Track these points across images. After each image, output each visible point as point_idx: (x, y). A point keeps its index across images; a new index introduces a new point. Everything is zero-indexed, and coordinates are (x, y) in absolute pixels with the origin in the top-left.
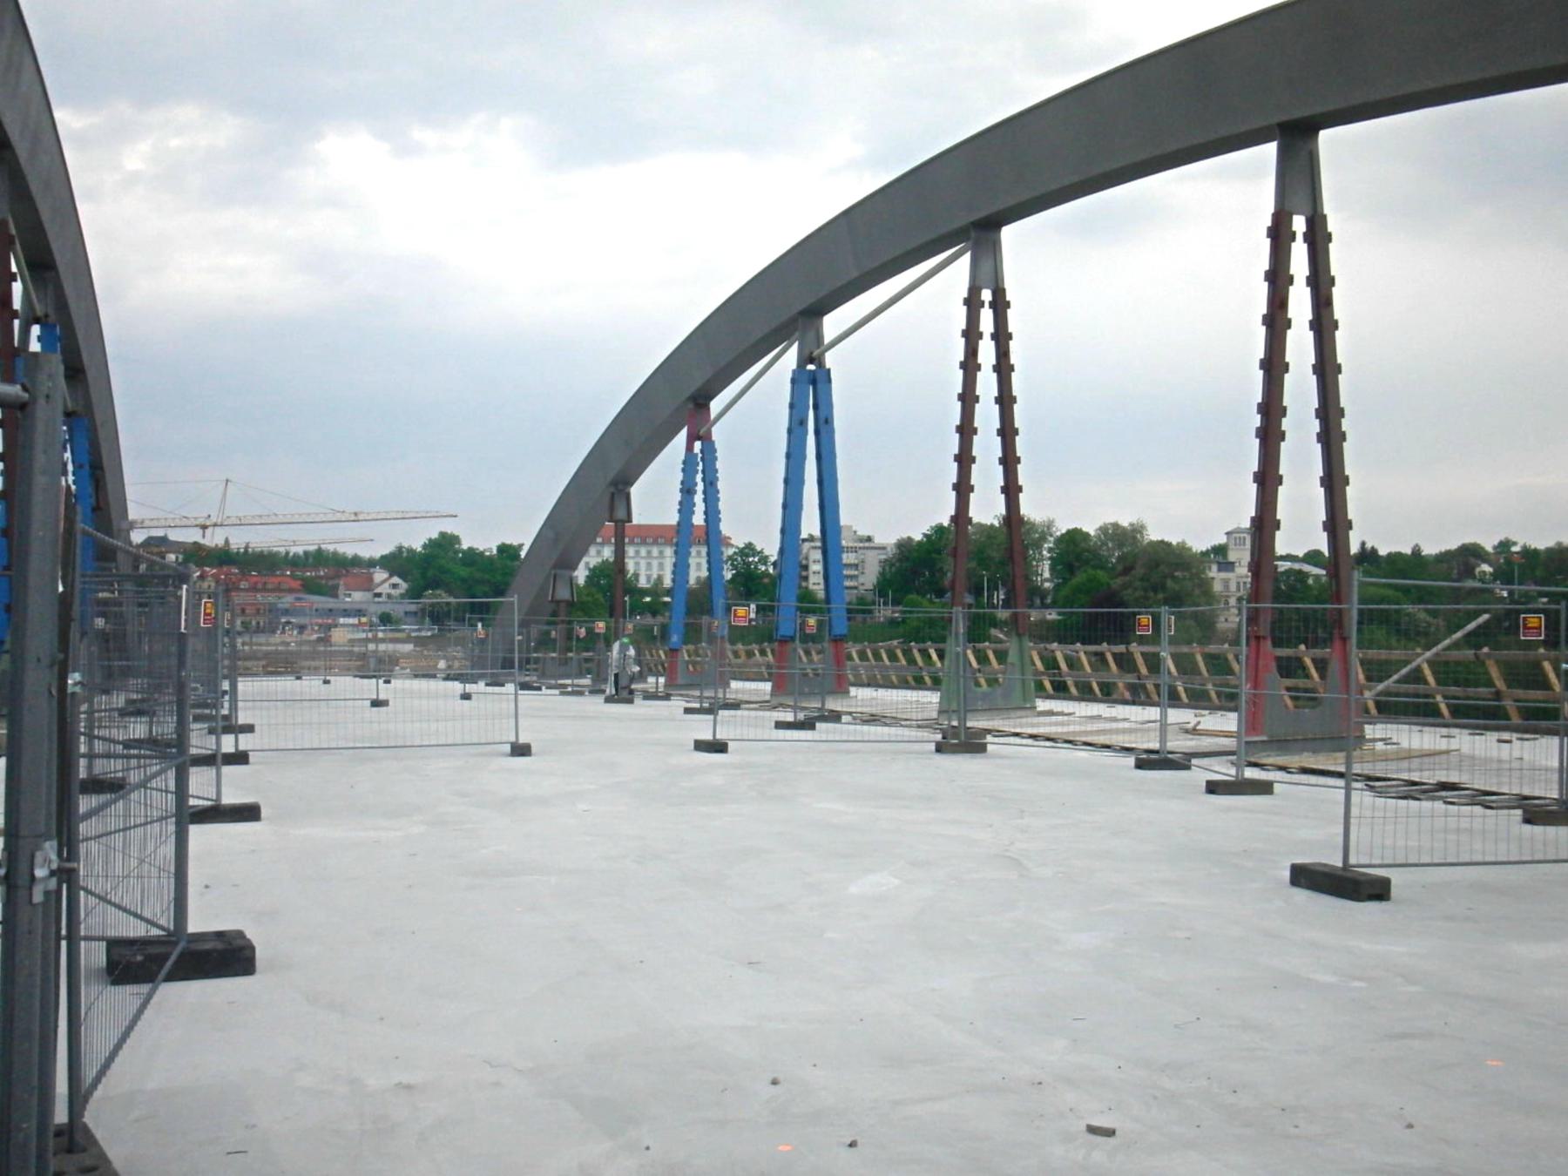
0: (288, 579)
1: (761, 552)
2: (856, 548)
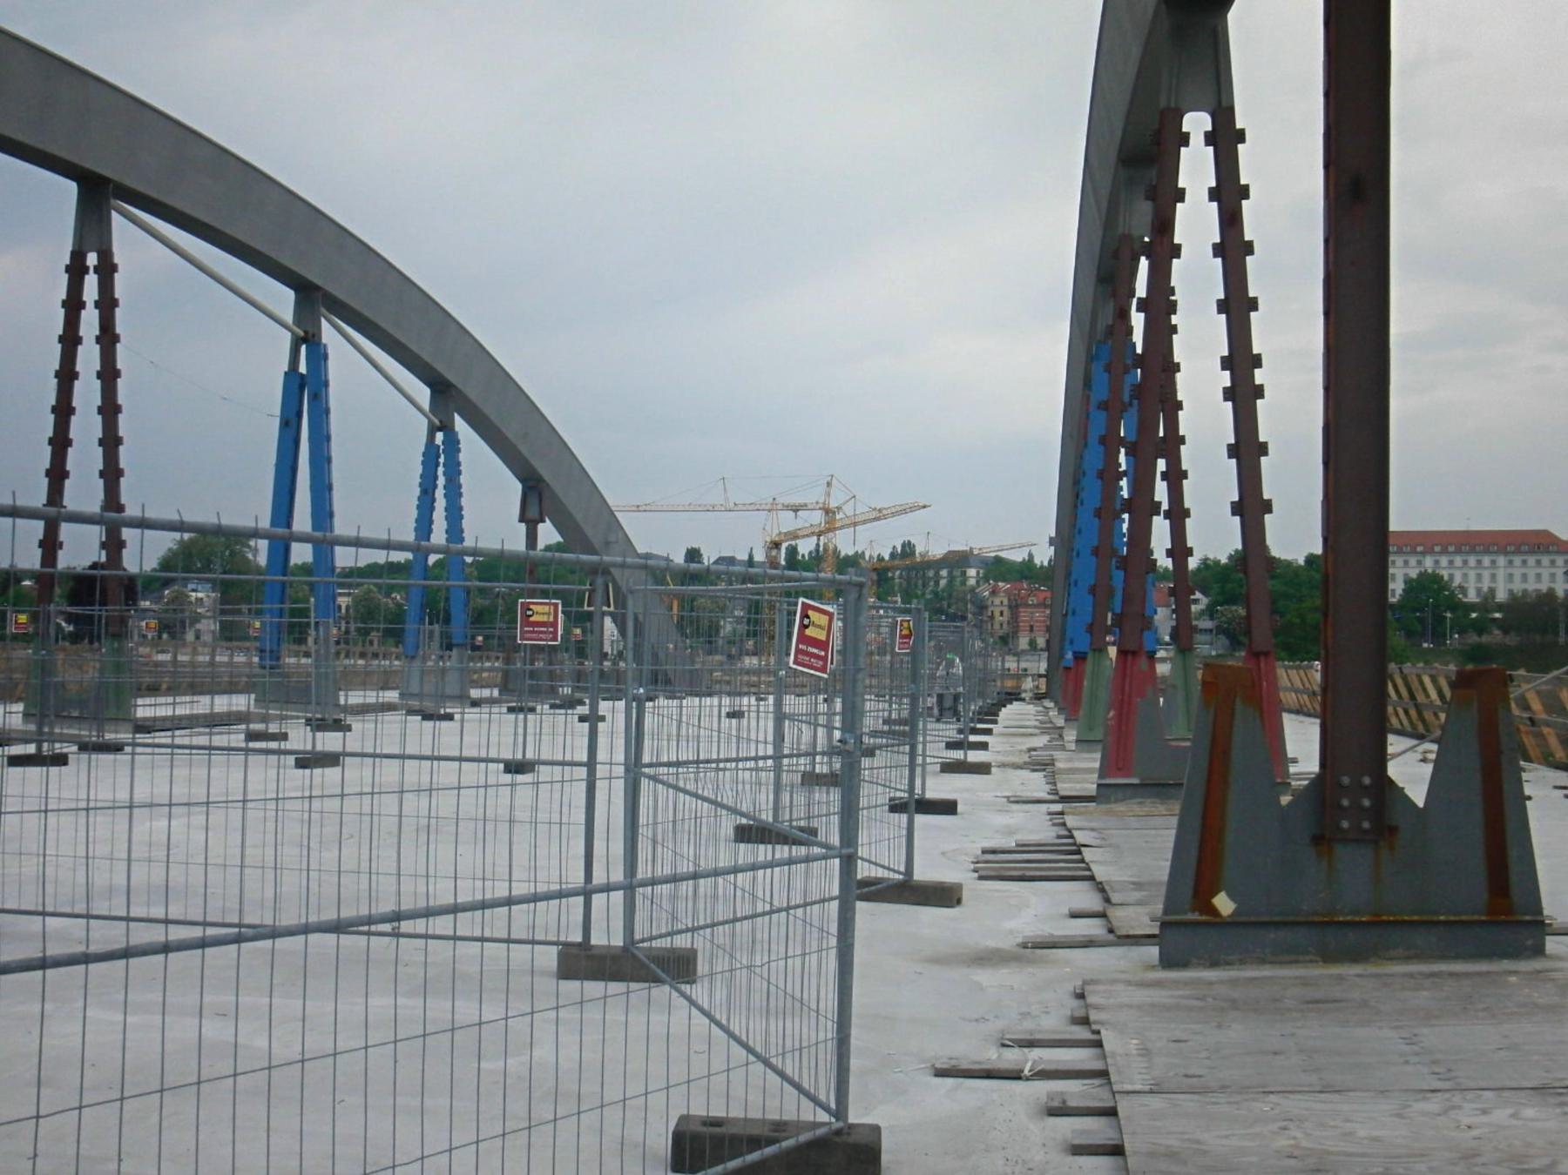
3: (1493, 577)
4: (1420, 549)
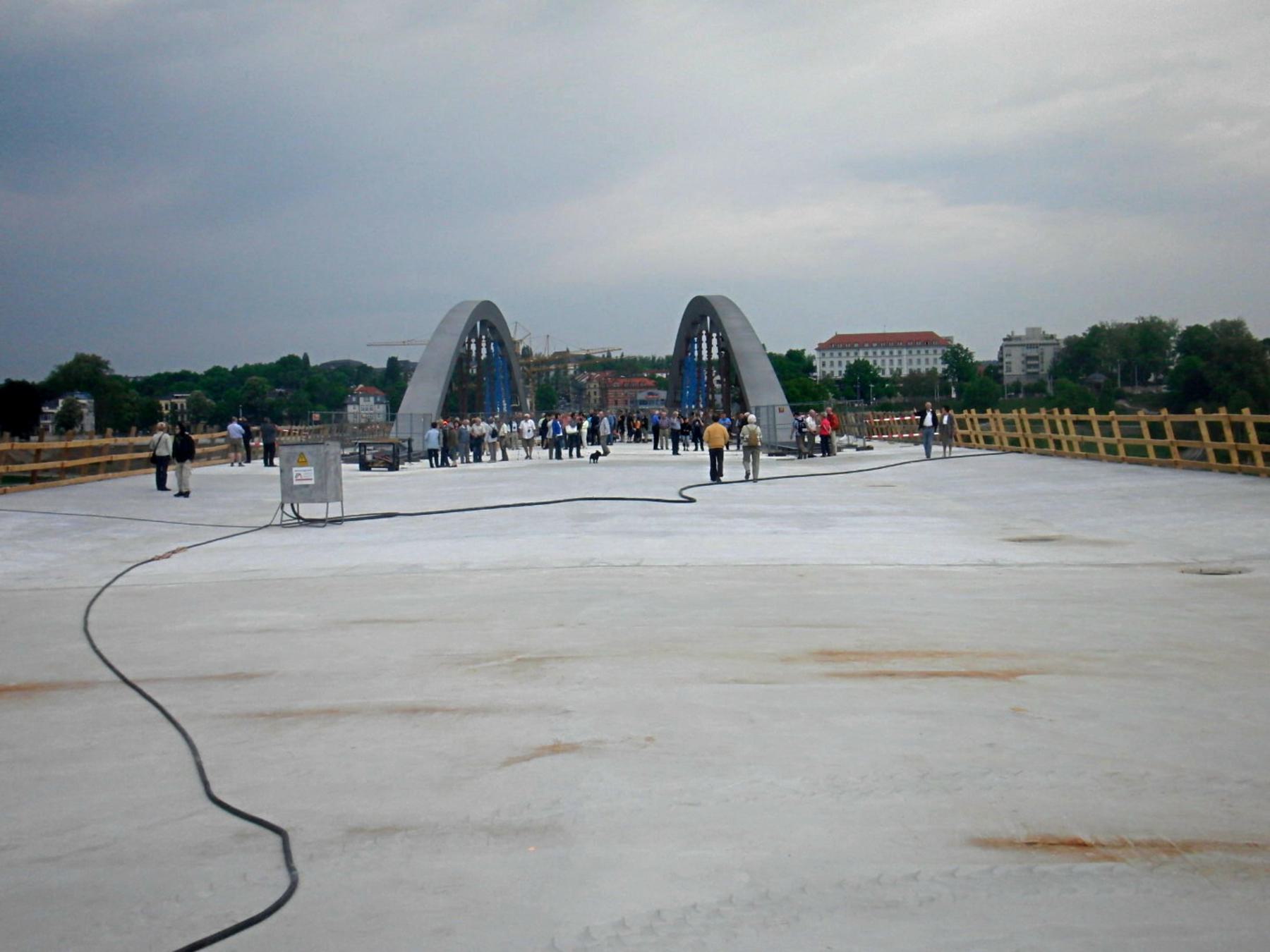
0: (646, 380)
1: (967, 350)
2: (1037, 344)
3: (900, 361)
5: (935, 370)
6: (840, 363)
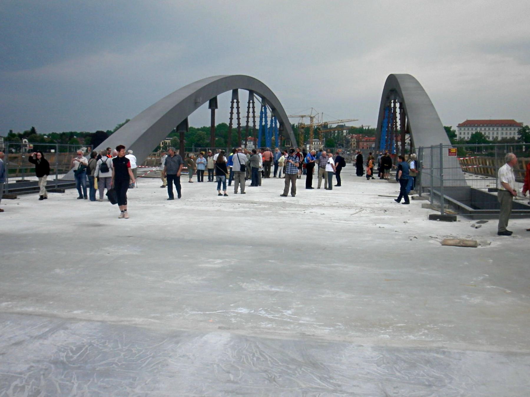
3: (497, 133)
4: (476, 125)
5: (514, 138)
6: (468, 133)
